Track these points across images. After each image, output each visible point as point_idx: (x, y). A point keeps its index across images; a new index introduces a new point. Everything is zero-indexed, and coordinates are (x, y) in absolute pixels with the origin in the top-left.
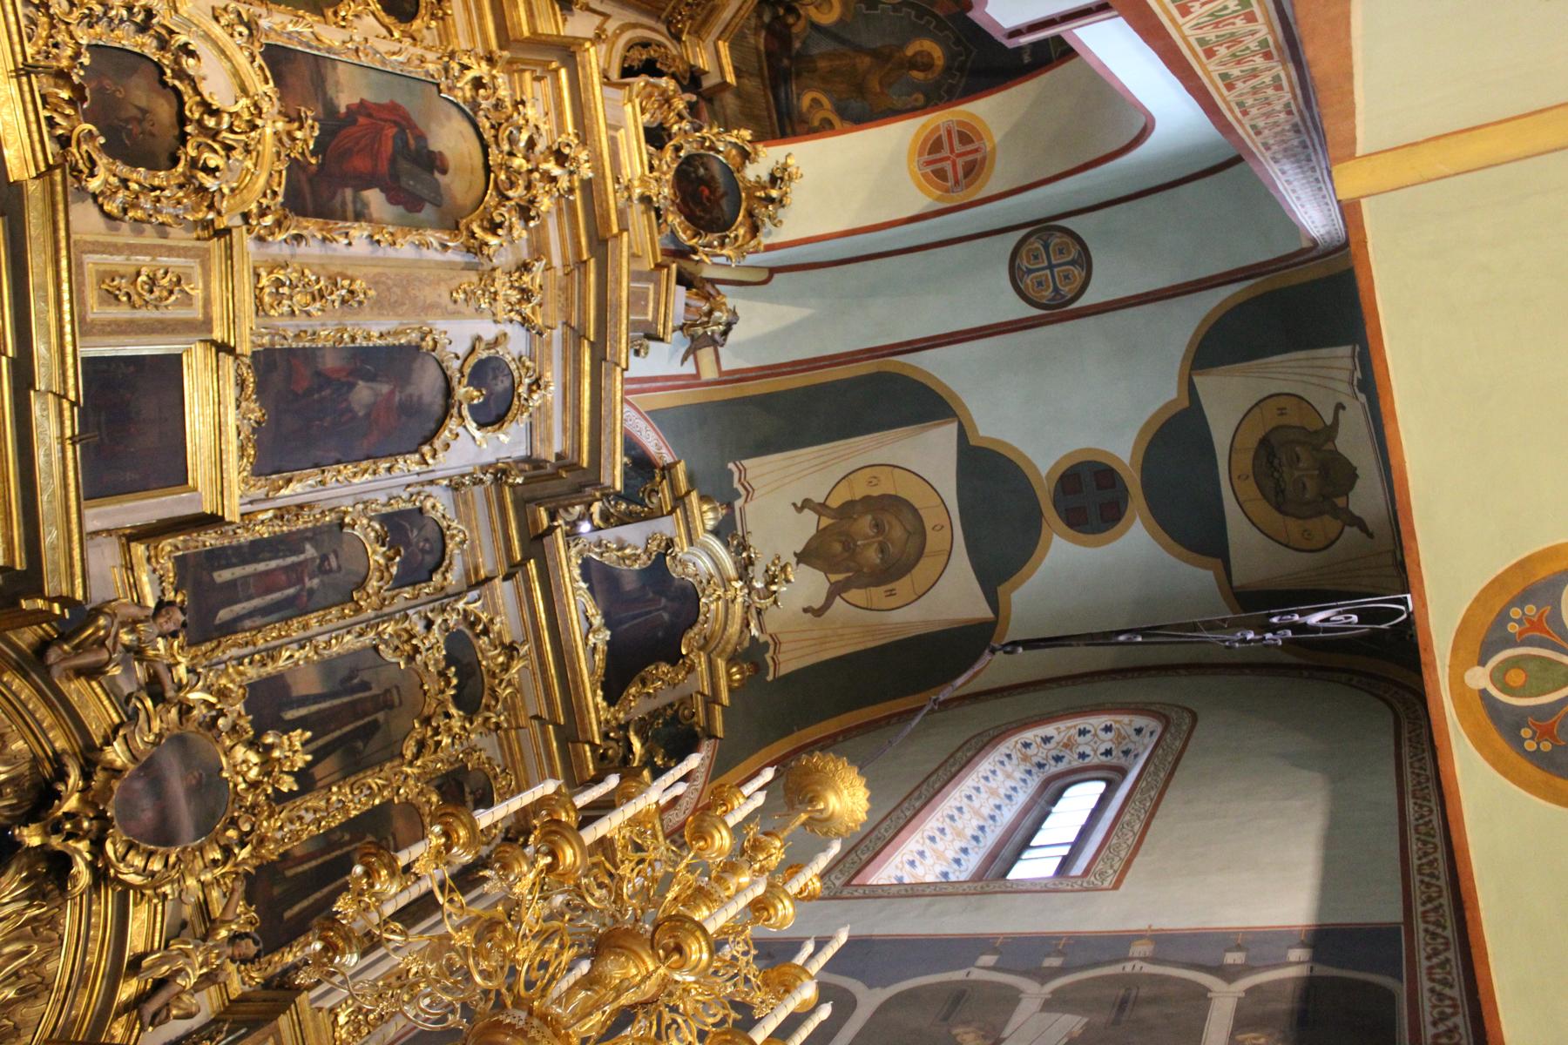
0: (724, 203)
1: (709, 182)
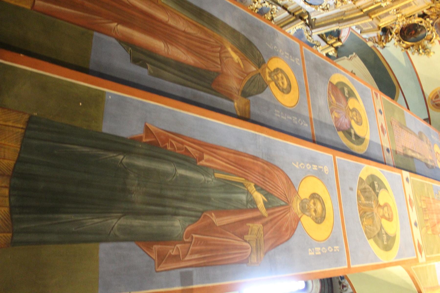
0: (412, 38)
1: (416, 32)
